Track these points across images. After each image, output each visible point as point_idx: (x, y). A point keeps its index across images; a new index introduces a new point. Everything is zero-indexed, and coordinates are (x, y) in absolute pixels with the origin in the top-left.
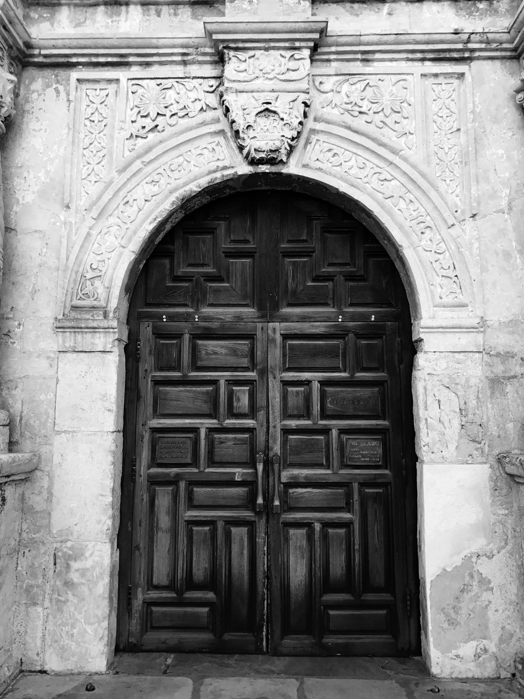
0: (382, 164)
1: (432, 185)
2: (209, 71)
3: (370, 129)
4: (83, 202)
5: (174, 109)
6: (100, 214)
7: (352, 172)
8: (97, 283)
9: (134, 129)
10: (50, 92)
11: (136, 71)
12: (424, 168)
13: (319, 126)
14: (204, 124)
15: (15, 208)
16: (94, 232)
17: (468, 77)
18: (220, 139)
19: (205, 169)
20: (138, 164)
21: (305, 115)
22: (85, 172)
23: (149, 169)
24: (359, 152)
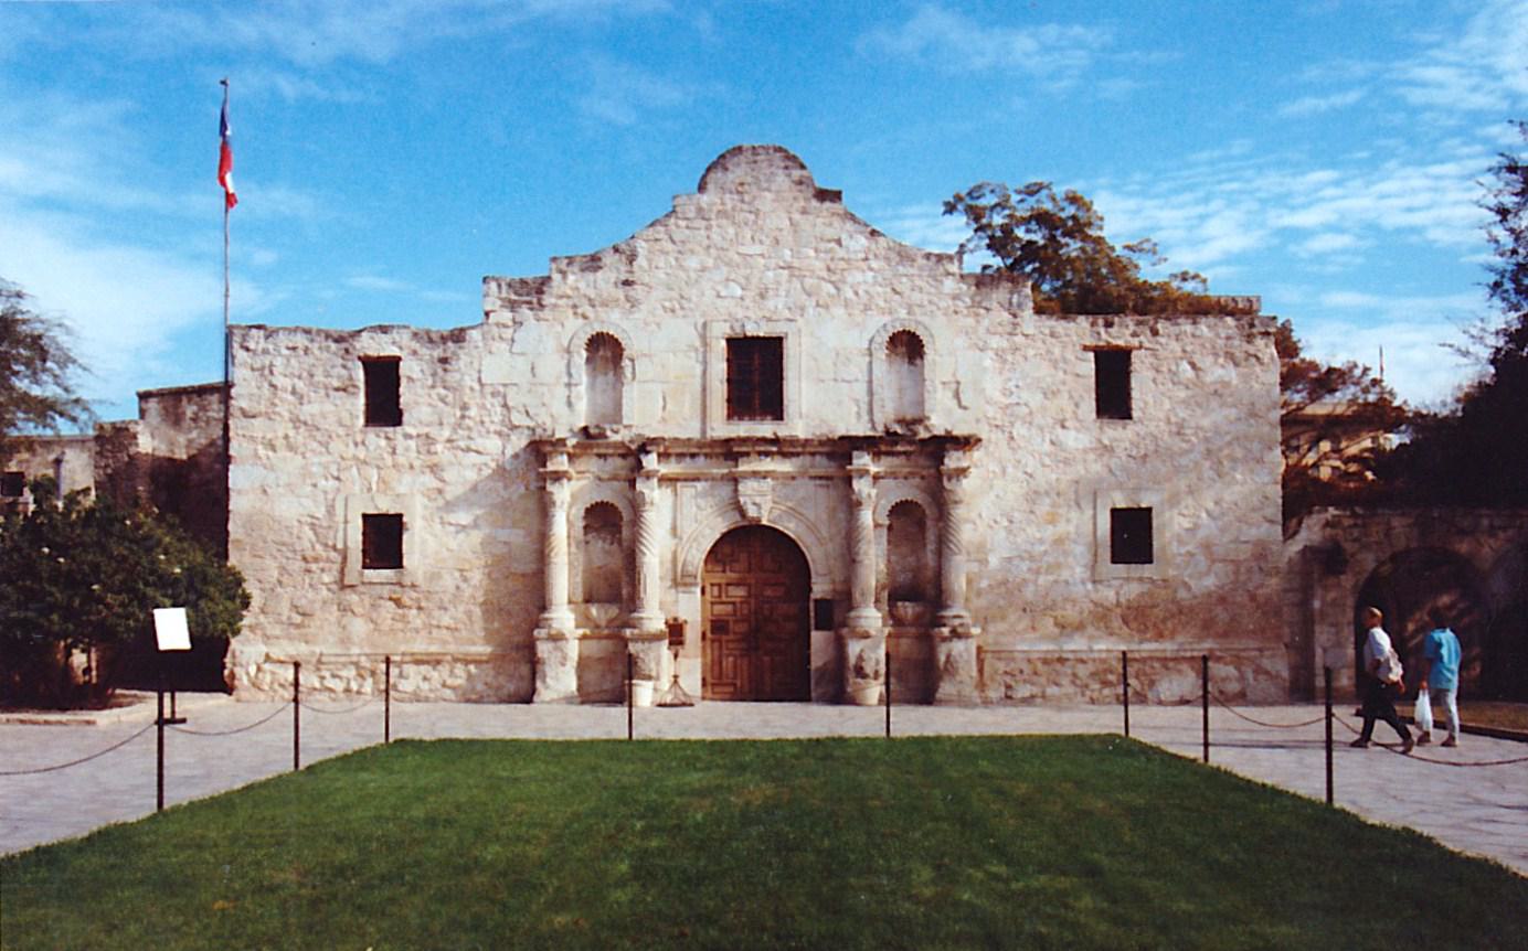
2: (732, 483)
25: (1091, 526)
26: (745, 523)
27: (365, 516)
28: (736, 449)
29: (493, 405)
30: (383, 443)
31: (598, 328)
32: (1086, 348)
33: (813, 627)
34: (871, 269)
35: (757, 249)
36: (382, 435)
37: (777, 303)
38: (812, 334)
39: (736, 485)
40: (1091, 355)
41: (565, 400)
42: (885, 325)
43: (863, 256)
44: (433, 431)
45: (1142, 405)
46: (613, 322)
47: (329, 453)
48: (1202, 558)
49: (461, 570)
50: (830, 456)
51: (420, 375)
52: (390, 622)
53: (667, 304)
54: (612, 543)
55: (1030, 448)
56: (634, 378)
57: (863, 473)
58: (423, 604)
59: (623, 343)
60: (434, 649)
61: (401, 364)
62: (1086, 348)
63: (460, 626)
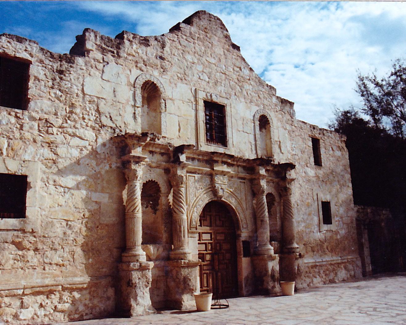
25: (317, 208)
26: (216, 199)
28: (215, 158)
29: (90, 109)
30: (13, 120)
31: (148, 78)
33: (242, 256)
36: (13, 114)
41: (132, 115)
42: (257, 111)
44: (52, 119)
51: (44, 78)
52: (11, 262)
53: (179, 75)
56: (166, 111)
58: (40, 246)
59: (162, 89)
60: (48, 282)
63: (66, 263)
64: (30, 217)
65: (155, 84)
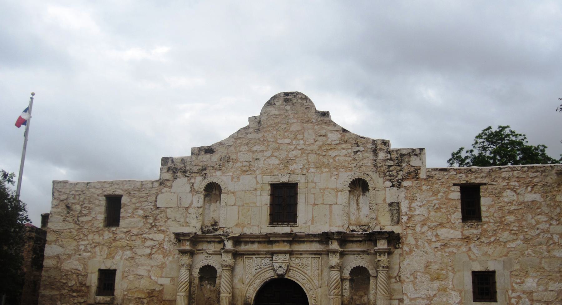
0: (303, 276)
1: (312, 280)
2: (270, 256)
3: (301, 269)
4: (246, 283)
5: (264, 264)
6: (250, 286)
7: (298, 278)
8: (249, 299)
9: (256, 268)
10: (240, 260)
11: (257, 256)
12: (312, 277)
13: (291, 268)
14: (269, 267)
15: (234, 284)
16: (249, 289)
17: (320, 258)
18: (273, 270)
19: (269, 276)
20: (257, 275)
21: (288, 267)
22: (247, 277)
23: (259, 277)
24: (299, 274)
26: (276, 277)
27: (100, 270)
28: (271, 239)
30: (111, 235)
32: (455, 185)
34: (343, 149)
35: (287, 141)
37: (296, 167)
38: (312, 182)
39: (272, 258)
40: (458, 188)
43: (338, 142)
45: (488, 214)
46: (216, 177)
47: (88, 240)
48: (527, 300)
49: (140, 298)
50: (320, 242)
53: (244, 168)
54: (214, 286)
55: (426, 238)
57: (334, 252)
61: (123, 198)
62: (455, 185)
64: (117, 296)
65: (217, 183)
